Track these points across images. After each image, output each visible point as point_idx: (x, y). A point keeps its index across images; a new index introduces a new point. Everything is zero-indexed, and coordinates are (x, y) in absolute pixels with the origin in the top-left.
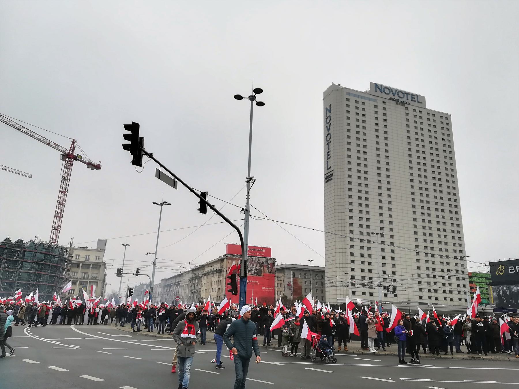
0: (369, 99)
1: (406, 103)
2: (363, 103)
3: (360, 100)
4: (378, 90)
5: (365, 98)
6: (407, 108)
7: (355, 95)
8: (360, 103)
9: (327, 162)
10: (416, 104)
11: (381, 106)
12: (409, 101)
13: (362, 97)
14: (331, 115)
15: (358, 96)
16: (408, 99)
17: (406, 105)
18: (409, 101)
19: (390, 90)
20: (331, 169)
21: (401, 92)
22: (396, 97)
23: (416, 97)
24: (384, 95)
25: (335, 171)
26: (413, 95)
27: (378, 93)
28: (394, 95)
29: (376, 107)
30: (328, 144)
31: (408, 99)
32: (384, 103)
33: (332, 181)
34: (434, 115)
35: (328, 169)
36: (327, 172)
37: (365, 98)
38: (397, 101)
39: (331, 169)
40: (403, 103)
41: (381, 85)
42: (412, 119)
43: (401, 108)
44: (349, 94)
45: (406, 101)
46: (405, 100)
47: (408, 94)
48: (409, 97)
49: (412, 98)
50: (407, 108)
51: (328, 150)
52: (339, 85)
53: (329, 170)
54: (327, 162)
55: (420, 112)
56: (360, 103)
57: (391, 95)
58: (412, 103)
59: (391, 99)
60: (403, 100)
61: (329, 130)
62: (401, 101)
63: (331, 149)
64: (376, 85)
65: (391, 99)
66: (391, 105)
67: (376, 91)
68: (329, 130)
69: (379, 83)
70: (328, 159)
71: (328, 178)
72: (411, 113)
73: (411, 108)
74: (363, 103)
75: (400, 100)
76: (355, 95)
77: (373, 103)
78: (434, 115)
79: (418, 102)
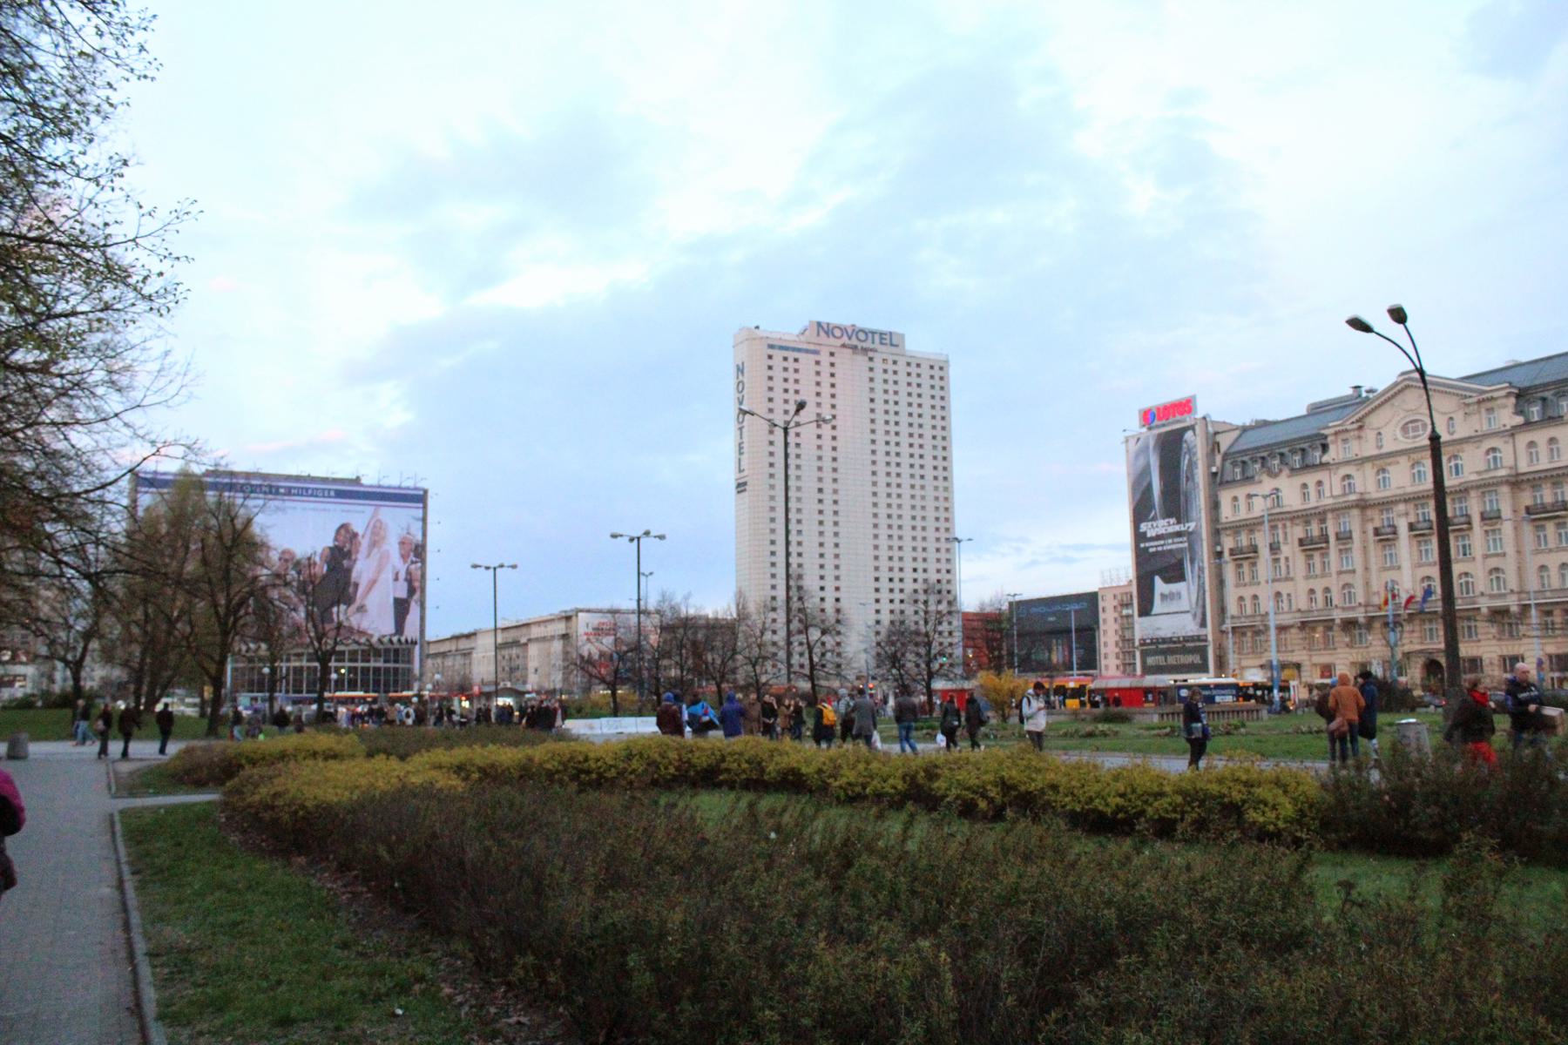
0: (807, 351)
1: (872, 350)
2: (796, 360)
3: (791, 355)
4: (822, 333)
5: (799, 350)
6: (871, 359)
7: (782, 348)
8: (791, 360)
11: (825, 358)
12: (877, 345)
13: (794, 349)
14: (745, 380)
15: (787, 349)
17: (871, 354)
18: (877, 345)
19: (843, 330)
21: (862, 330)
22: (854, 342)
23: (888, 337)
24: (832, 341)
26: (881, 334)
27: (823, 338)
28: (850, 338)
29: (818, 363)
30: (741, 429)
32: (832, 354)
34: (918, 365)
36: (738, 475)
37: (799, 350)
38: (854, 348)
39: (745, 473)
40: (865, 350)
41: (828, 324)
42: (879, 376)
43: (862, 360)
44: (771, 347)
45: (872, 346)
46: (868, 345)
47: (873, 333)
48: (877, 337)
49: (881, 339)
50: (871, 359)
52: (757, 327)
55: (895, 362)
56: (791, 360)
57: (845, 340)
59: (844, 346)
60: (865, 345)
62: (862, 349)
63: (745, 439)
64: (819, 324)
65: (844, 346)
66: (844, 359)
67: (818, 334)
69: (824, 319)
70: (741, 454)
71: (741, 487)
72: (878, 365)
73: (878, 358)
74: (796, 360)
75: (860, 345)
76: (782, 348)
77: (813, 357)
78: (918, 365)
79: (892, 345)
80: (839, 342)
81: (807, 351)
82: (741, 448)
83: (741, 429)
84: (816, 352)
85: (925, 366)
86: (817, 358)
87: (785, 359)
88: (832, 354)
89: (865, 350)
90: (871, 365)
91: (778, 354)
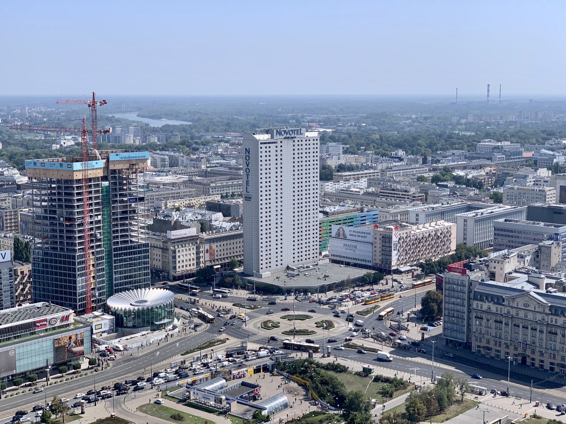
0: (272, 143)
2: (270, 147)
3: (268, 145)
10: (299, 136)
16: (295, 134)
17: (294, 140)
18: (296, 135)
20: (250, 194)
22: (288, 136)
25: (253, 196)
28: (287, 134)
30: (248, 175)
31: (295, 134)
33: (250, 202)
35: (247, 192)
36: (246, 193)
43: (291, 141)
44: (261, 143)
46: (293, 136)
49: (297, 132)
50: (294, 141)
53: (248, 193)
57: (285, 135)
58: (297, 136)
59: (285, 138)
61: (248, 166)
65: (285, 138)
68: (248, 166)
70: (247, 185)
72: (296, 143)
73: (296, 140)
74: (270, 147)
80: (284, 137)
81: (272, 143)
82: (247, 183)
83: (248, 175)
85: (311, 140)
86: (276, 145)
88: (281, 142)
89: (292, 138)
90: (294, 144)
91: (263, 146)
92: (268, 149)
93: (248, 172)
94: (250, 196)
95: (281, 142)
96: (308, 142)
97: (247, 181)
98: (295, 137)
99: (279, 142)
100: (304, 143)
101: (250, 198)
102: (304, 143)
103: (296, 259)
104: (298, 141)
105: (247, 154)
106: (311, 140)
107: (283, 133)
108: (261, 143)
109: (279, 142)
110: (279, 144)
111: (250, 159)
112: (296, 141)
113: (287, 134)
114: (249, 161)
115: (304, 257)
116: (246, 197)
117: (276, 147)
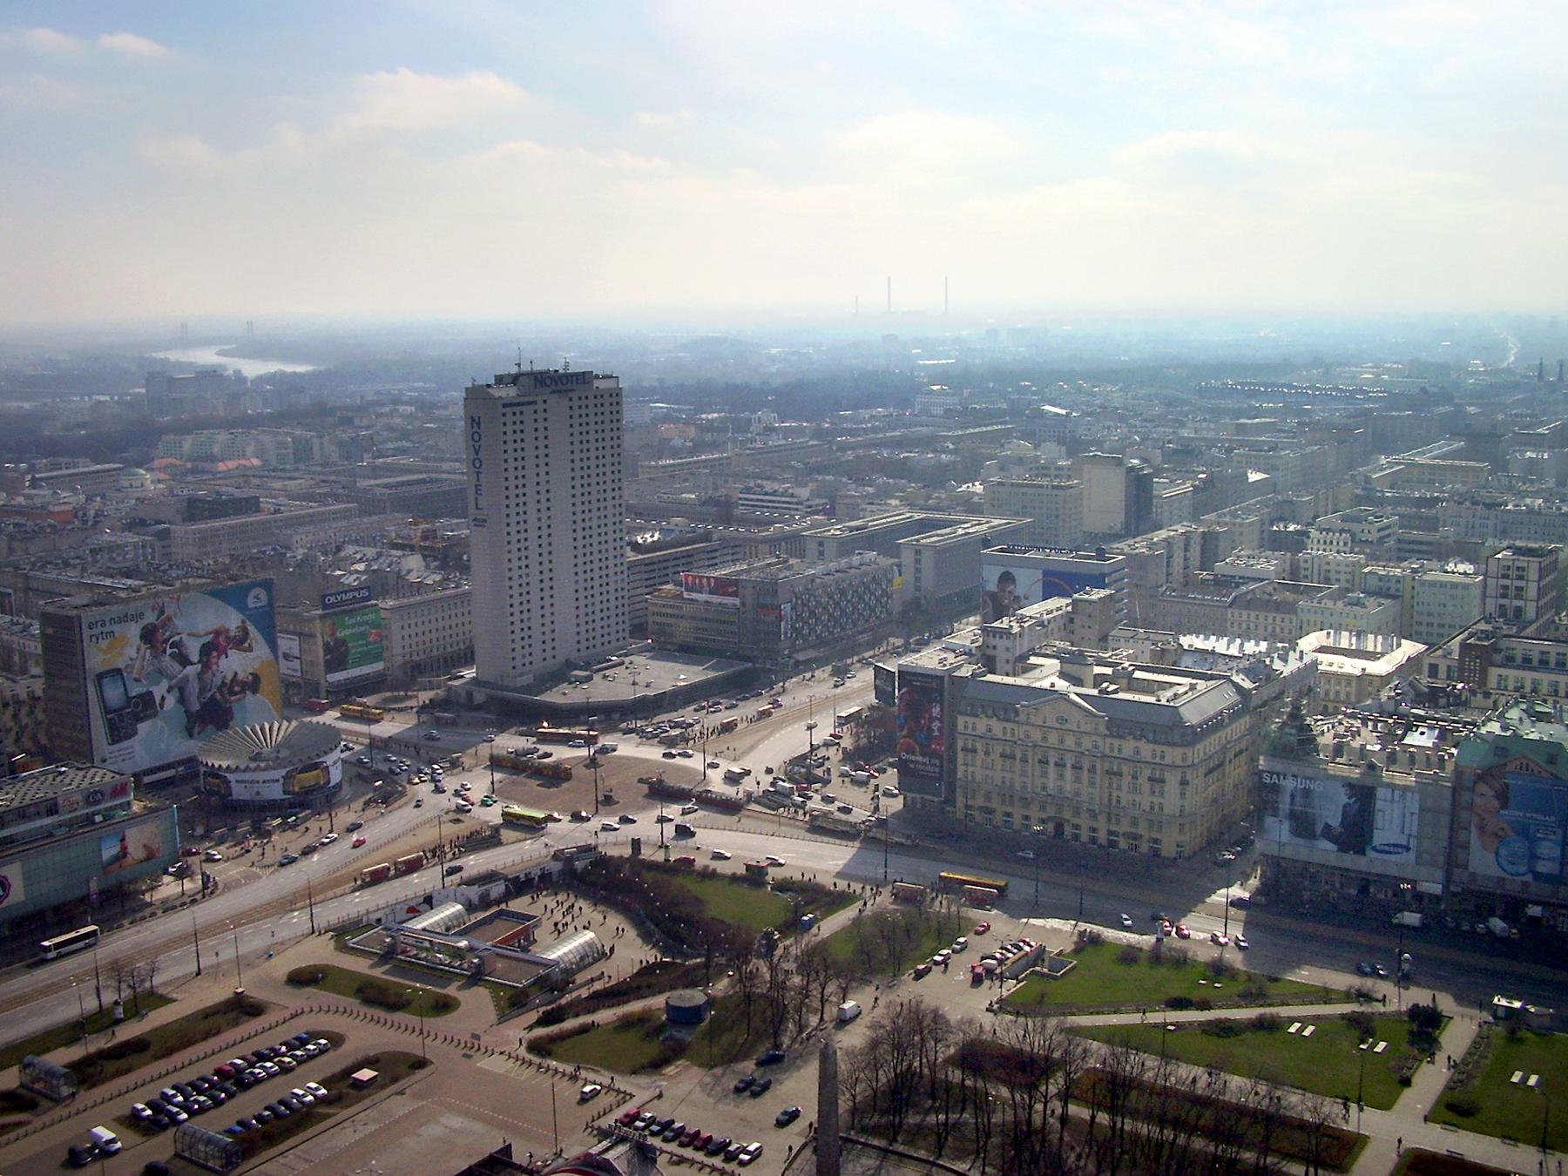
1: (570, 390)
9: (476, 499)
12: (574, 387)
17: (571, 395)
22: (560, 387)
28: (556, 384)
30: (478, 473)
35: (477, 508)
44: (505, 406)
46: (569, 386)
49: (577, 379)
50: (571, 399)
51: (478, 480)
53: (480, 511)
54: (476, 499)
59: (554, 392)
72: (576, 403)
77: (532, 407)
80: (550, 389)
82: (477, 490)
83: (478, 473)
84: (535, 403)
85: (606, 396)
87: (514, 414)
88: (545, 402)
91: (509, 410)
92: (518, 418)
93: (478, 465)
94: (484, 517)
95: (545, 402)
96: (599, 401)
97: (476, 486)
98: (573, 390)
99: (540, 402)
100: (591, 401)
101: (485, 521)
102: (591, 401)
103: (584, 644)
104: (580, 398)
105: (476, 429)
106: (606, 396)
107: (548, 382)
108: (505, 406)
109: (540, 402)
110: (540, 407)
111: (483, 437)
112: (575, 399)
113: (556, 384)
114: (482, 443)
115: (598, 641)
116: (475, 520)
117: (536, 412)
